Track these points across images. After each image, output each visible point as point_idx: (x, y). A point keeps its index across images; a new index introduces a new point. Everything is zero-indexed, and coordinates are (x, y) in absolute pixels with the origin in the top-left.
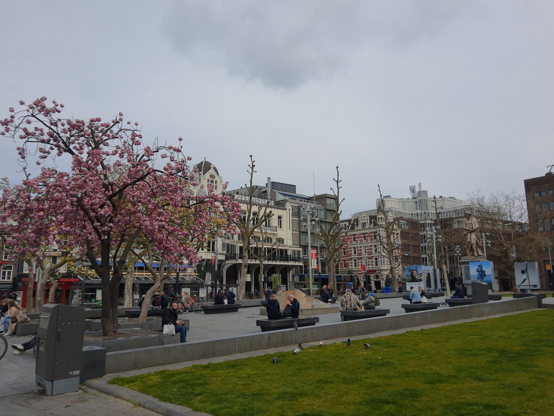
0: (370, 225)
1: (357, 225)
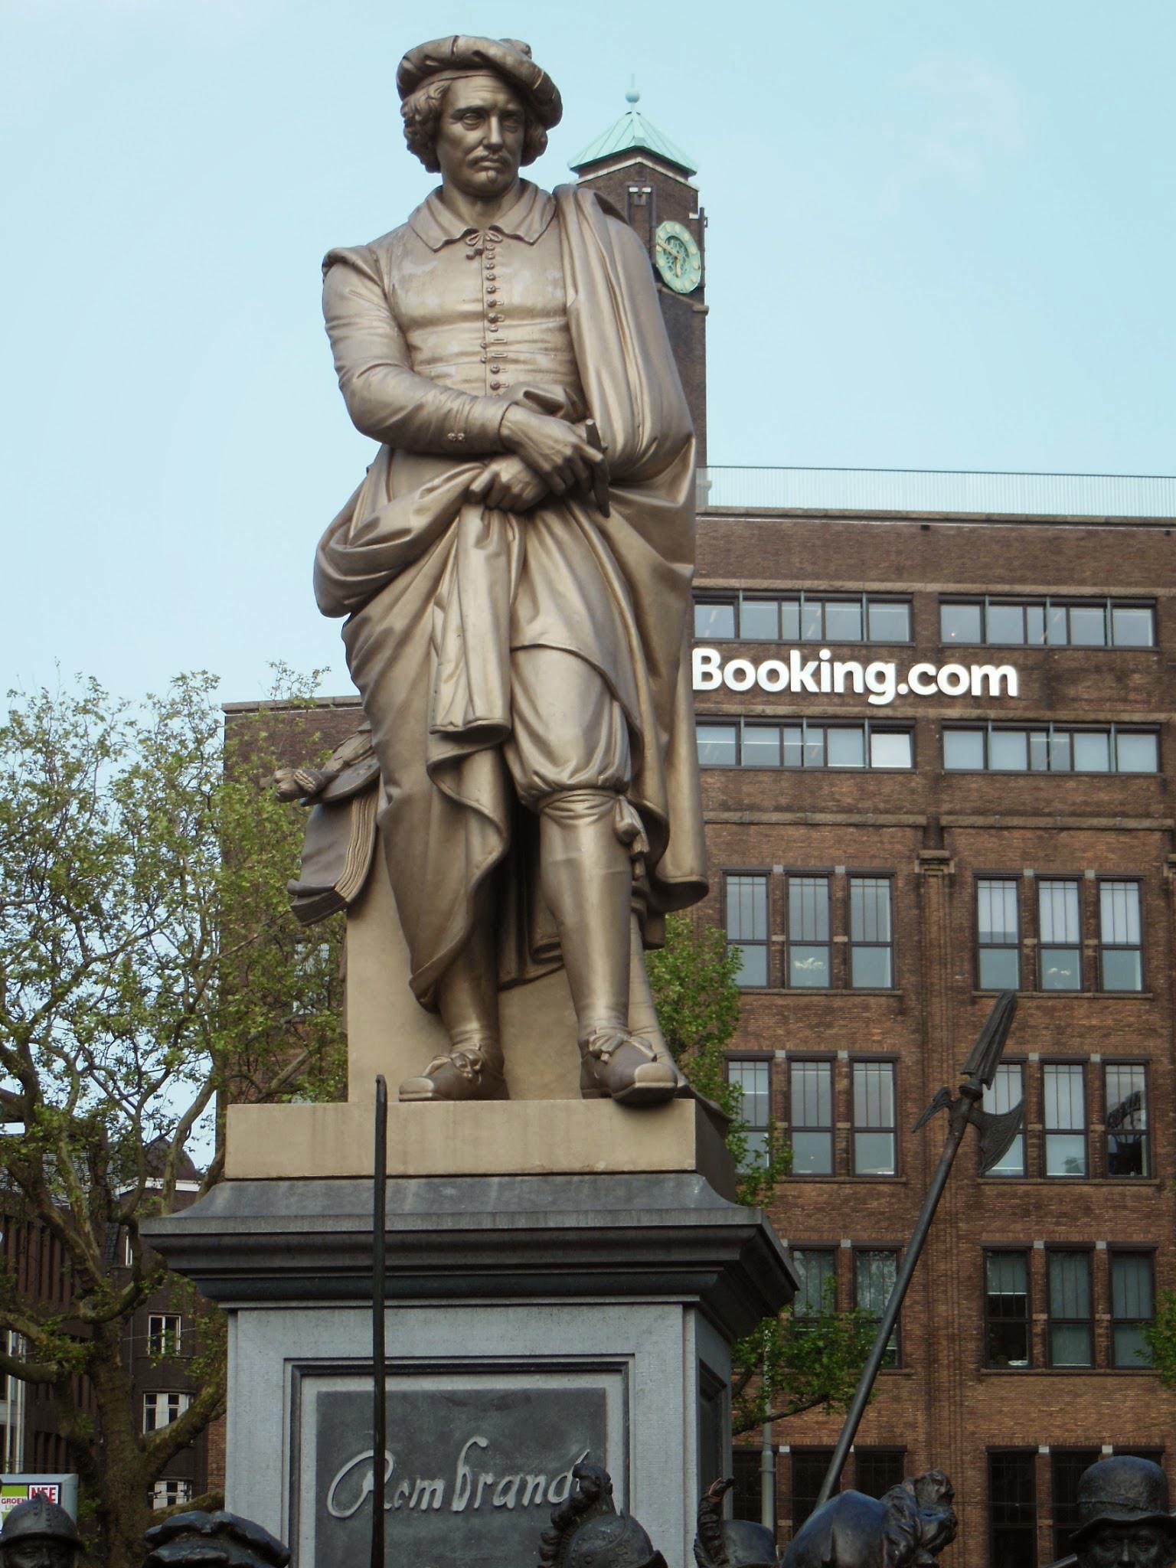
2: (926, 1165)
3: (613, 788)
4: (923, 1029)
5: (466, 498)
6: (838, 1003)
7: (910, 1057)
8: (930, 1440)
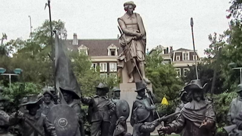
3: (144, 61)
5: (132, 39)
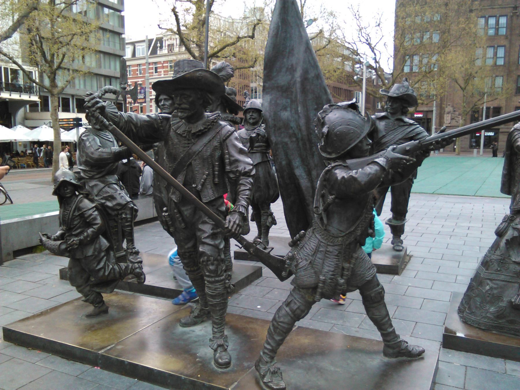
0: (179, 48)
1: (161, 47)
2: (509, 63)
4: (510, 41)
6: (496, 37)
7: (508, 46)
8: (506, 105)
